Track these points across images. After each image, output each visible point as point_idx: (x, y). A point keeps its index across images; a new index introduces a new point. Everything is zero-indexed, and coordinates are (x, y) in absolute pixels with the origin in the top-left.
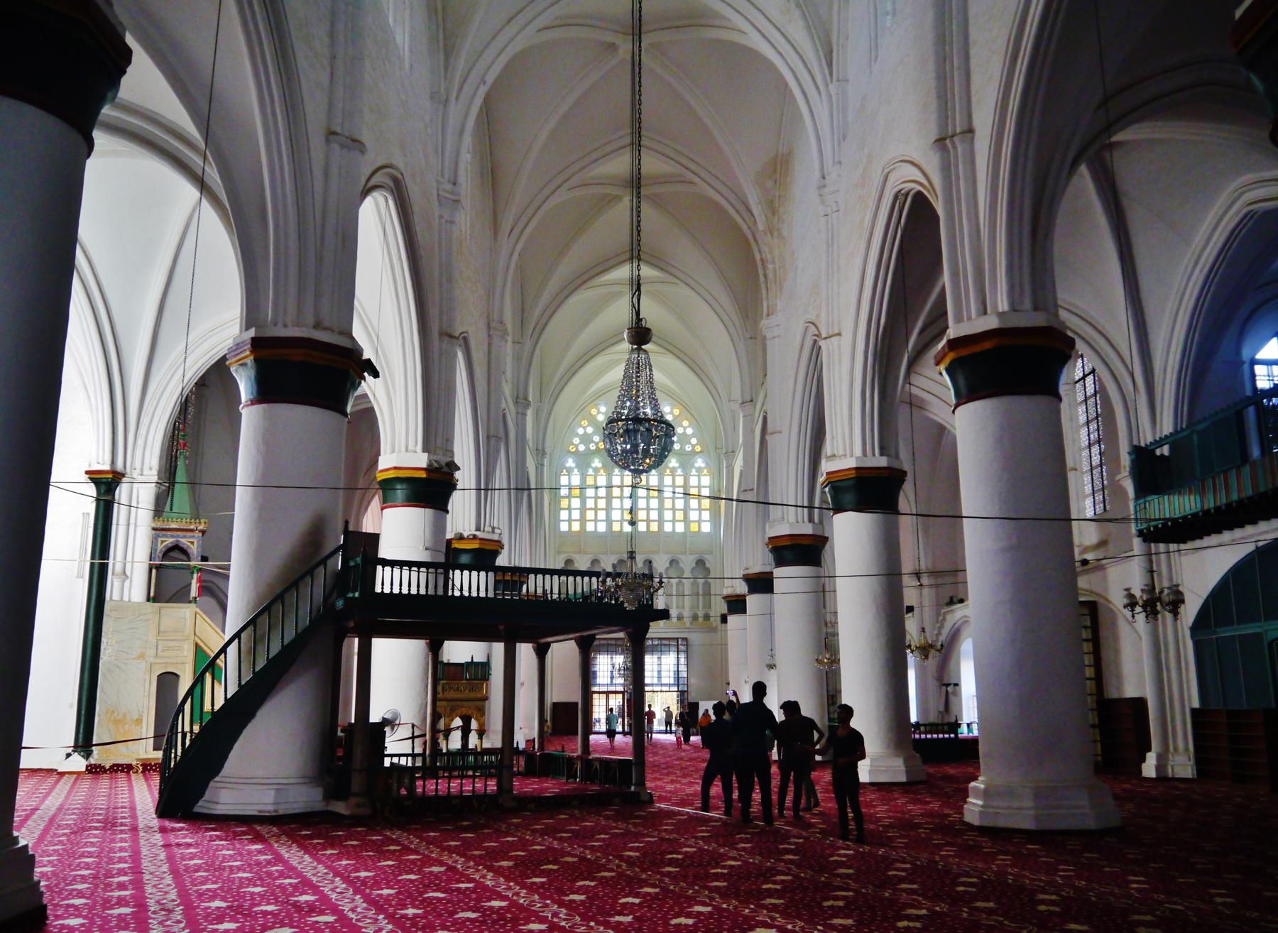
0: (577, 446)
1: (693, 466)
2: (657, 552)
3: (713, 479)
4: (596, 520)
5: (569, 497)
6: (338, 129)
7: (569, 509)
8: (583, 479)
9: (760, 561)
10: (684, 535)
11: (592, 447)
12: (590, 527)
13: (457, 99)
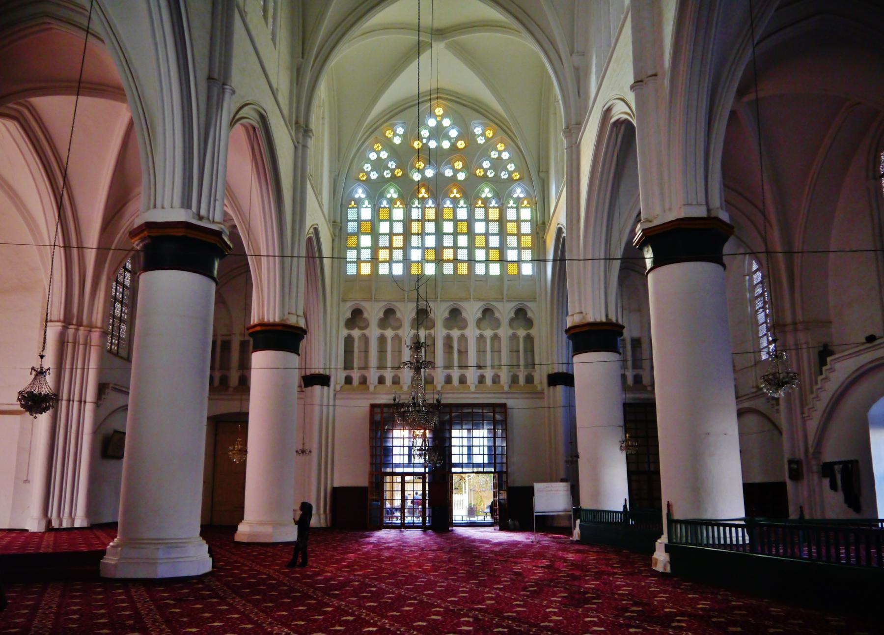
0: (368, 174)
1: (510, 196)
2: (467, 299)
4: (390, 261)
5: (358, 233)
7: (358, 248)
10: (500, 278)
11: (387, 174)
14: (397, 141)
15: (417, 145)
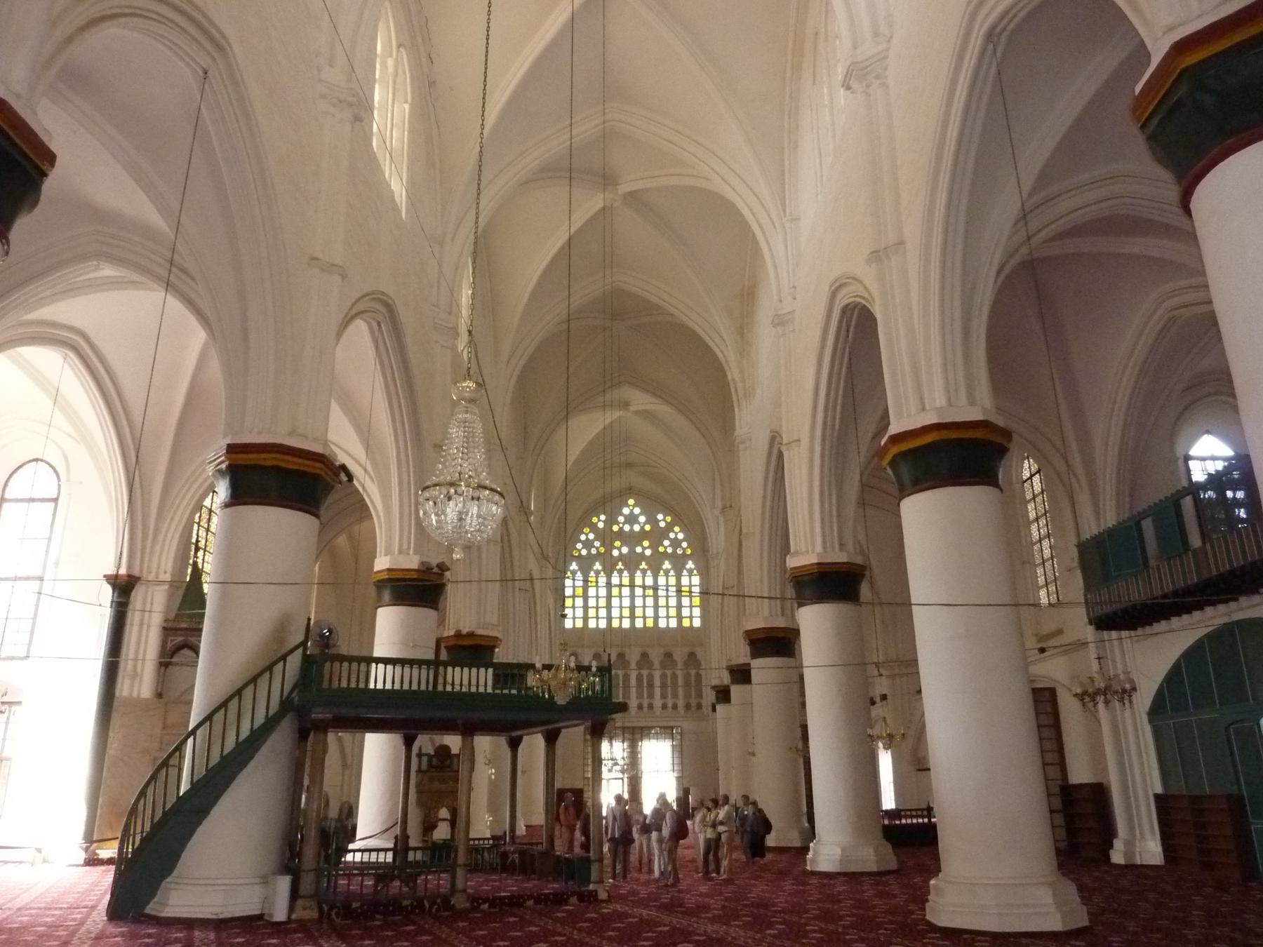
3: (701, 580)
5: (574, 597)
6: (320, 256)
8: (586, 581)
9: (741, 653)
12: (592, 624)
13: (453, 240)
14: (601, 525)
15: (615, 528)
